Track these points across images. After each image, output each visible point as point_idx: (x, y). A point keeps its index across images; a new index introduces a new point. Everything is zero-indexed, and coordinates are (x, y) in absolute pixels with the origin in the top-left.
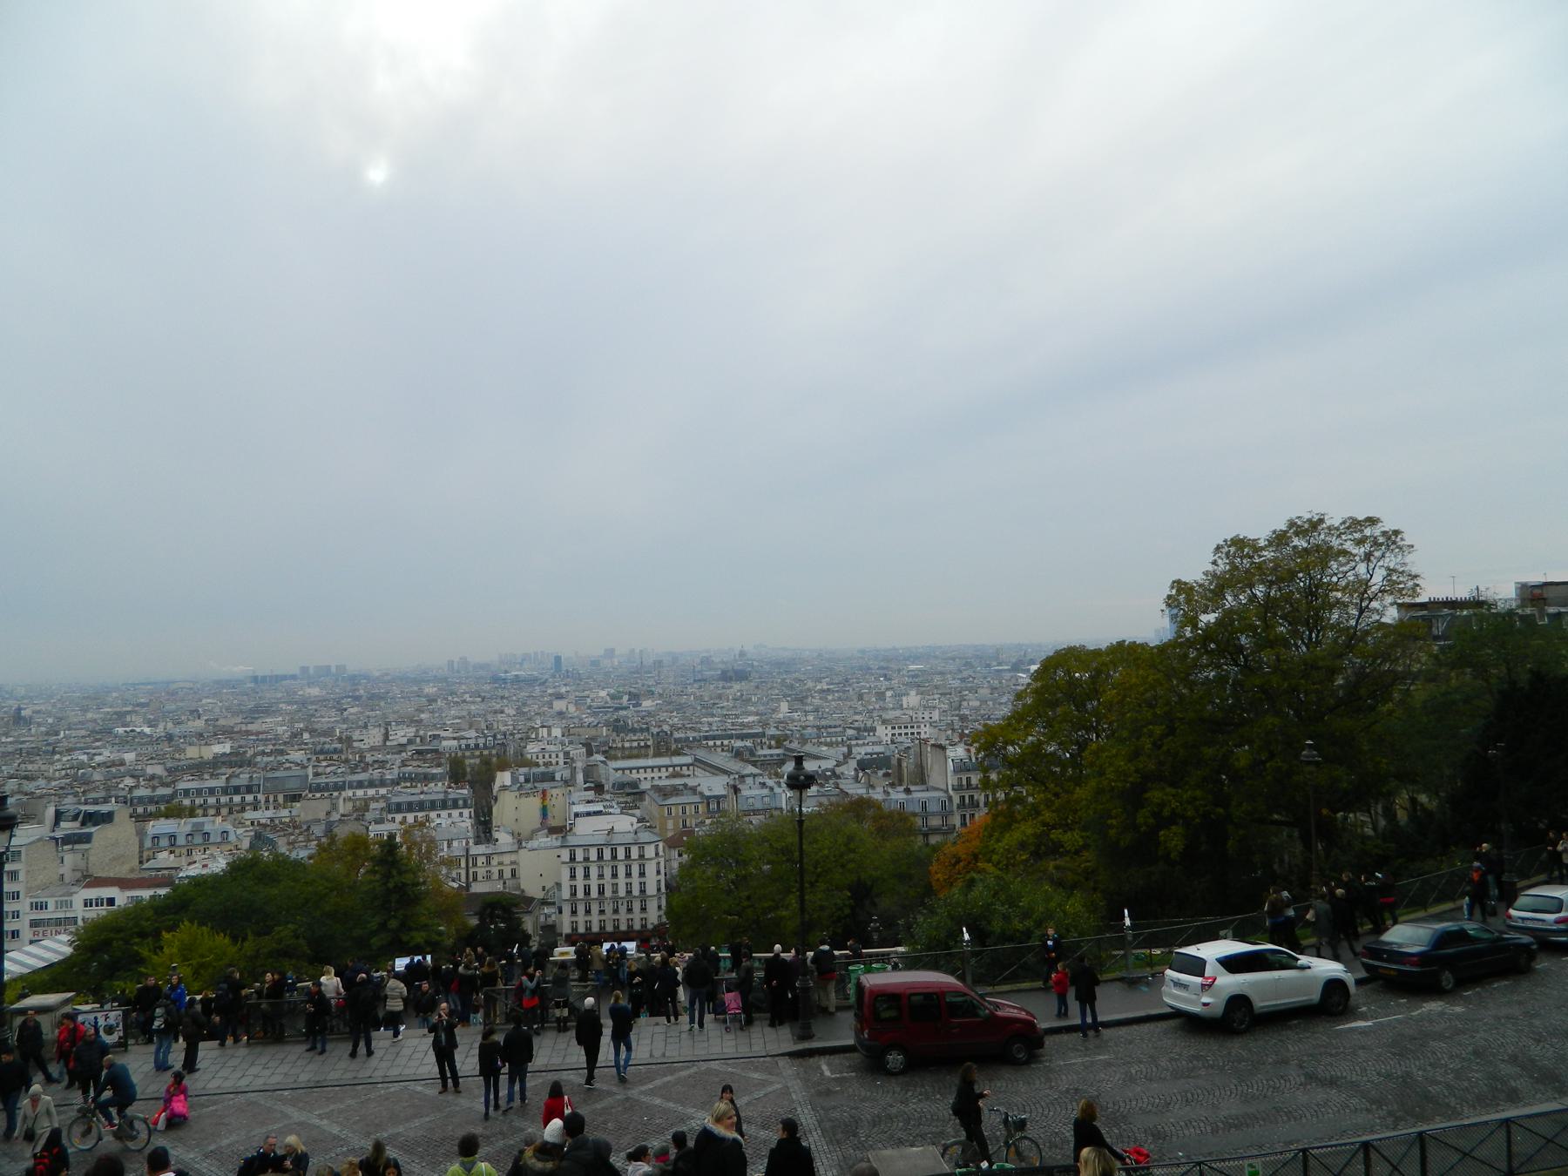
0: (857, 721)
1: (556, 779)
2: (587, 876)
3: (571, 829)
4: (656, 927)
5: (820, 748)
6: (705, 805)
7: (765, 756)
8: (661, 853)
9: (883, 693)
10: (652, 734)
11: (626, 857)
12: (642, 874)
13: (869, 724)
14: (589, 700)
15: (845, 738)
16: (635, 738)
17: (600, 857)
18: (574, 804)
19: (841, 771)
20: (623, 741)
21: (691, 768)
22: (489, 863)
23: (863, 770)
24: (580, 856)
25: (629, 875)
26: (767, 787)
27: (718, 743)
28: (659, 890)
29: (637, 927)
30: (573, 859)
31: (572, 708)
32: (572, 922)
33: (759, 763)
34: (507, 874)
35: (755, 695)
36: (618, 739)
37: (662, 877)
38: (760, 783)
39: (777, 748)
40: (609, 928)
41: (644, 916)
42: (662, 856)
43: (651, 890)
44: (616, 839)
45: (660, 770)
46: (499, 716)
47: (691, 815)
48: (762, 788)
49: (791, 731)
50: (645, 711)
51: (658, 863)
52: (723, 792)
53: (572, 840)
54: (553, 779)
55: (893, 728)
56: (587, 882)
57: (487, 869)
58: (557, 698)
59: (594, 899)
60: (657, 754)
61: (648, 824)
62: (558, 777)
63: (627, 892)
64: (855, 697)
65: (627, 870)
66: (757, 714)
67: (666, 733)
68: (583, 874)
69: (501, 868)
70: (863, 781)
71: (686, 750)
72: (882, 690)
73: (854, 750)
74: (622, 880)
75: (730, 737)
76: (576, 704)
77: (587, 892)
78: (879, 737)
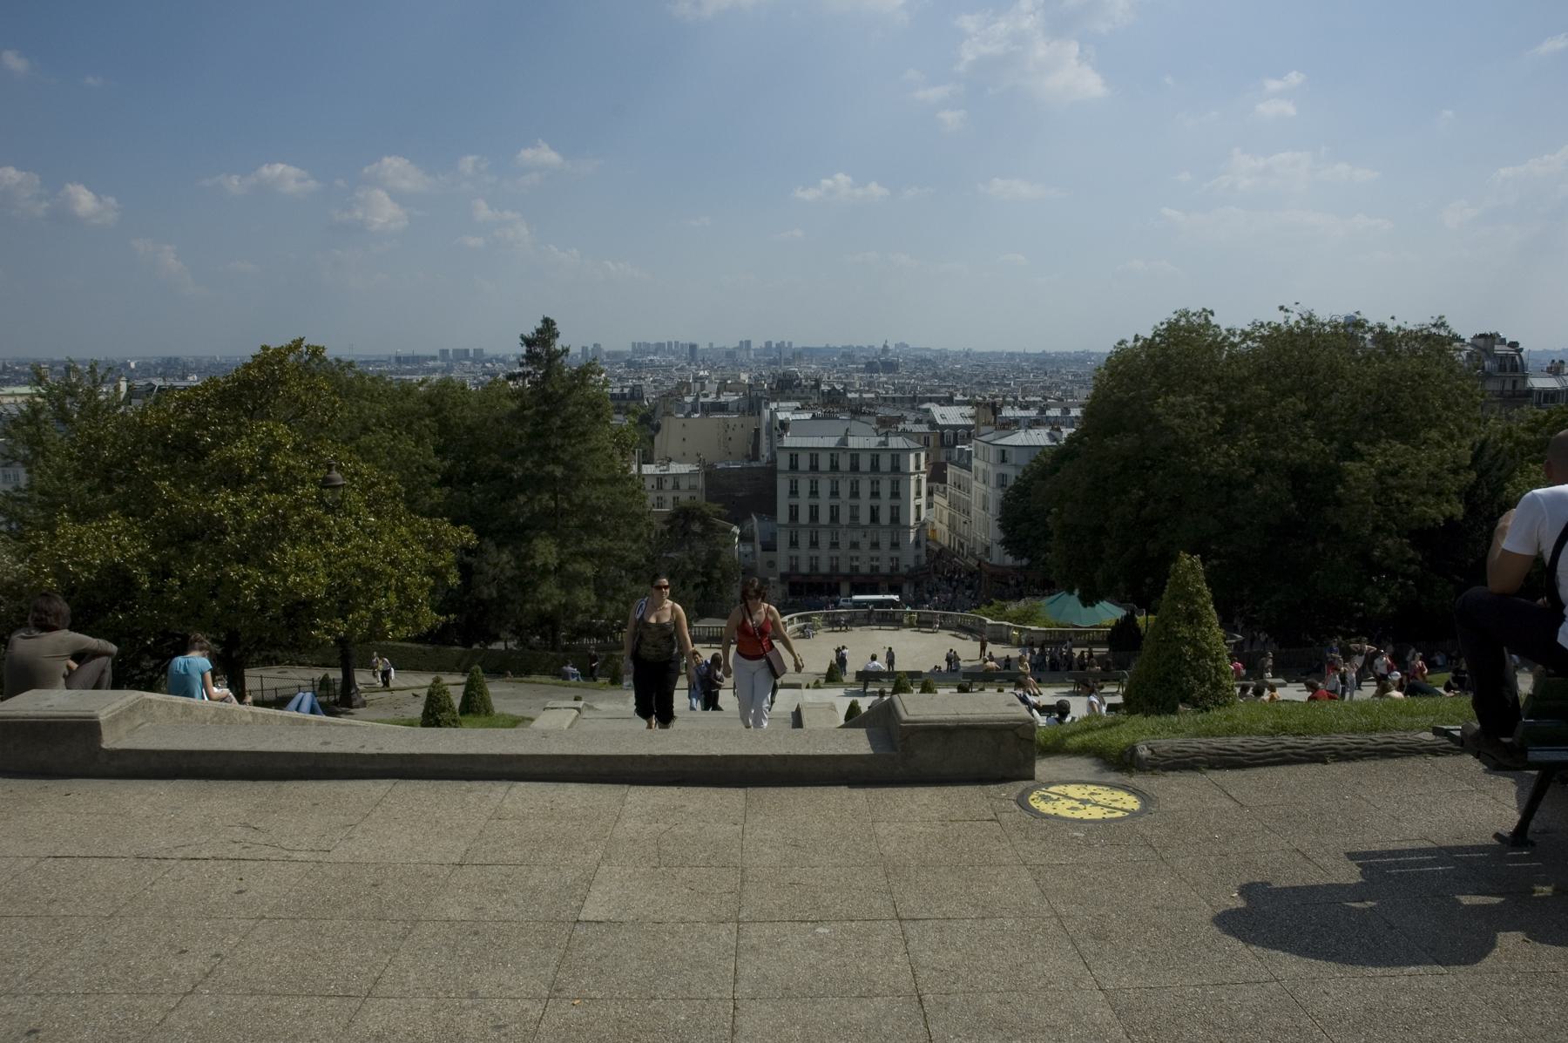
2: (814, 493)
8: (923, 468)
22: (660, 487)
24: (804, 463)
25: (875, 495)
41: (895, 554)
42: (924, 472)
44: (853, 443)
51: (919, 481)
52: (961, 422)
56: (813, 501)
57: (659, 495)
59: (824, 526)
68: (808, 489)
69: (676, 495)
77: (814, 513)
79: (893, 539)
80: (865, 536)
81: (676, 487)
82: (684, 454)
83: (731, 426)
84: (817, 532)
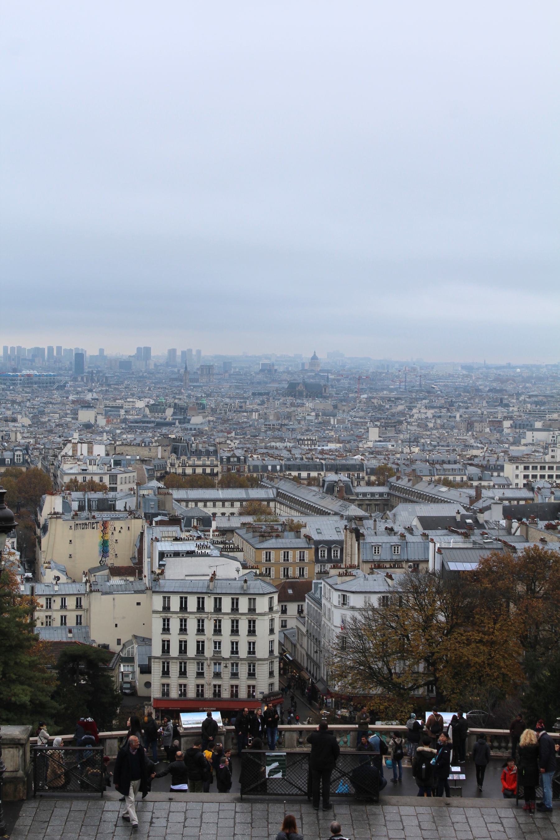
0: (476, 456)
1: (117, 508)
2: (183, 630)
3: (162, 573)
4: (266, 699)
5: (437, 488)
6: (313, 550)
7: (365, 494)
8: (275, 609)
9: (500, 422)
10: (222, 459)
11: (232, 610)
12: (252, 632)
13: (493, 462)
14: (122, 412)
15: (465, 478)
16: (200, 463)
17: (201, 608)
18: (157, 540)
19: (486, 519)
20: (184, 465)
21: (272, 504)
22: (49, 606)
23: (519, 520)
25: (235, 631)
26: (395, 534)
27: (304, 474)
28: (271, 652)
29: (243, 694)
30: (166, 609)
31: (102, 421)
32: (163, 685)
33: (357, 502)
34: (71, 622)
35: (334, 416)
36: (177, 462)
37: (276, 637)
38: (386, 528)
39: (379, 485)
40: (208, 694)
41: (252, 682)
42: (277, 612)
43: (262, 652)
45: (232, 505)
46: (11, 424)
47: (294, 563)
48: (389, 535)
49: (398, 464)
50: (195, 429)
51: (272, 620)
52: (335, 537)
53: (166, 585)
54: (112, 508)
55: (526, 468)
56: (183, 637)
58: (82, 407)
60: (227, 484)
61: (258, 573)
62: (120, 505)
63: (232, 652)
64: (463, 426)
65: (233, 626)
66: (339, 442)
67: (239, 458)
69: (64, 613)
70: (518, 533)
71: (265, 482)
72: (499, 419)
73: (485, 493)
74: (226, 638)
75: (319, 468)
76: (107, 415)
77: (183, 649)
78: (507, 478)
79: (250, 670)
80: (226, 667)
81: (63, 606)
82: (70, 555)
83: (118, 529)
84: (185, 663)
